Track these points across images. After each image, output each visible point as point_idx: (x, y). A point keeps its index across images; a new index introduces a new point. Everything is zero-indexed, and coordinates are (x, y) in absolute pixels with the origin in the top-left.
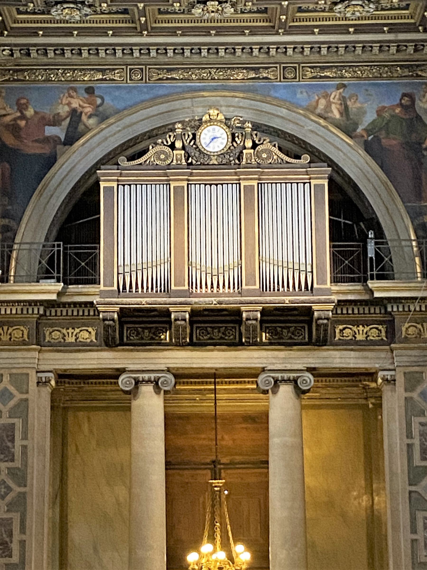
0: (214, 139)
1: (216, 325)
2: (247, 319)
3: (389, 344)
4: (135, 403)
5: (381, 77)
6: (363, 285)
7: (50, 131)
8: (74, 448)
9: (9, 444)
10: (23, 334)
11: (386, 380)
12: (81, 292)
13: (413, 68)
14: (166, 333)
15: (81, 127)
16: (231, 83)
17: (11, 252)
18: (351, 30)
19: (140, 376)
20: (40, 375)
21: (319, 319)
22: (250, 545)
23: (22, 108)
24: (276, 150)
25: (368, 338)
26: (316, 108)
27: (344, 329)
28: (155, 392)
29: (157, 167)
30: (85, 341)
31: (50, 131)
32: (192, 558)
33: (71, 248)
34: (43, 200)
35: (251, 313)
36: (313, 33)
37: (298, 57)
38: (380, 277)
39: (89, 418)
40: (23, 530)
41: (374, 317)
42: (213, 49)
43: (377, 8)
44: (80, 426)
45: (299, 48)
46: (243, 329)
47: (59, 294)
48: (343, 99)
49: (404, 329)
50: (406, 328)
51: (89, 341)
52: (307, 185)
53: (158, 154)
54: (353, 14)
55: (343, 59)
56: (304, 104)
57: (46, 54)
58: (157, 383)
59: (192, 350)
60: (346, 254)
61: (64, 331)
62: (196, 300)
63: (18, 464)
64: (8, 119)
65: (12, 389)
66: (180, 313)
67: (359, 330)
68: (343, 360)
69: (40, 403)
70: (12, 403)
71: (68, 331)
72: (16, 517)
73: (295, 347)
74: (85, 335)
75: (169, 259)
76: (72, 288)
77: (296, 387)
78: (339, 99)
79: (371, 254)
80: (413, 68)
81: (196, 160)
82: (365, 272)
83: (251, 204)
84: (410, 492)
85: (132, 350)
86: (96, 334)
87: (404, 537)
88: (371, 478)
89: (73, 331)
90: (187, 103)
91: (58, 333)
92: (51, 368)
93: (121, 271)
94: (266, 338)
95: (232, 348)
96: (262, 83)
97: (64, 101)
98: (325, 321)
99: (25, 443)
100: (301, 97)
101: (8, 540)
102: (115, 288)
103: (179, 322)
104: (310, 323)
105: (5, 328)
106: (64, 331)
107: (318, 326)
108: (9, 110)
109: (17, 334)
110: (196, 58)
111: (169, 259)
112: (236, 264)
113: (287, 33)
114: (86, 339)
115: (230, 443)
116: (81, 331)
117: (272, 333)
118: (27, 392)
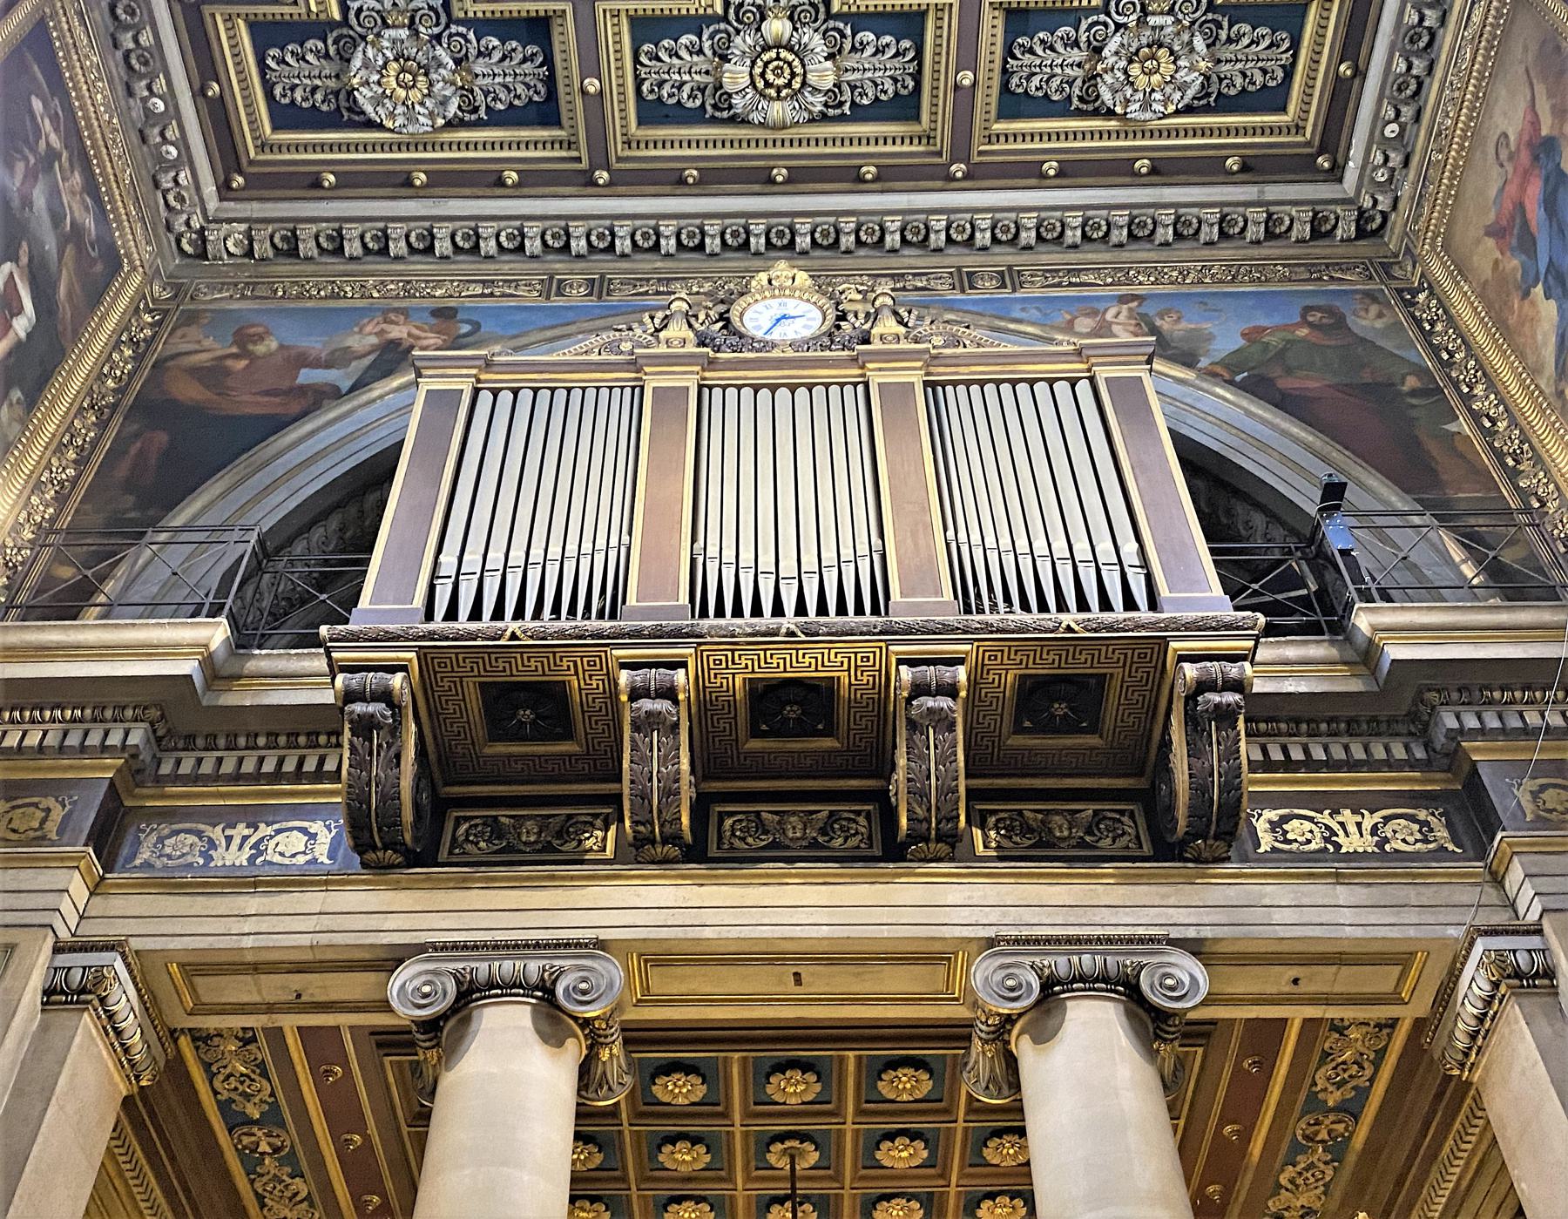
1: (796, 760)
2: (920, 689)
3: (1481, 855)
6: (1332, 642)
10: (44, 821)
12: (297, 678)
14: (607, 830)
20: (63, 960)
25: (1387, 847)
27: (1285, 819)
28: (538, 1032)
30: (287, 861)
47: (208, 662)
51: (301, 860)
67: (1342, 824)
71: (229, 832)
73: (1108, 868)
75: (625, 538)
78: (1130, 318)
89: (246, 832)
91: (191, 839)
94: (985, 847)
95: (857, 869)
98: (1231, 698)
103: (646, 705)
108: (208, 343)
111: (625, 538)
112: (863, 549)
114: (293, 856)
116: (278, 832)
117: (1009, 829)
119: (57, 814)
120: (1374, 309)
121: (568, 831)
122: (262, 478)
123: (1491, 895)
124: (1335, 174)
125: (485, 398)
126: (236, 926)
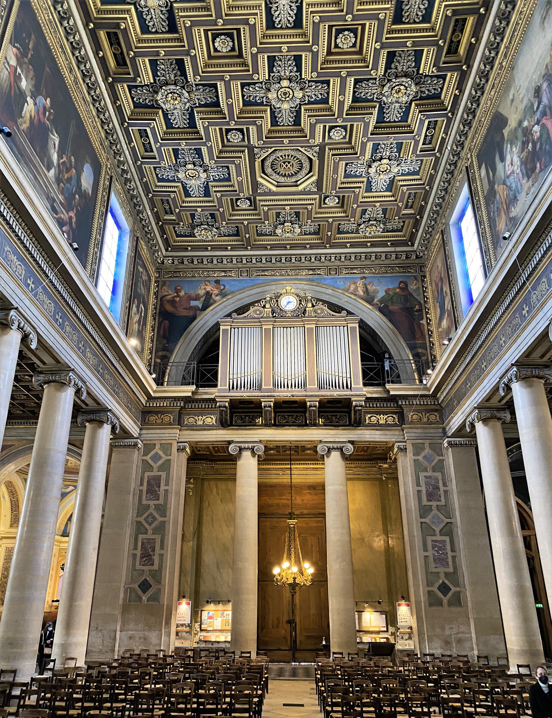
0: (289, 303)
1: (291, 412)
2: (310, 406)
3: (401, 426)
4: (239, 463)
5: (387, 273)
7: (193, 303)
8: (207, 503)
9: (157, 489)
11: (400, 449)
13: (405, 268)
15: (212, 301)
16: (299, 277)
17: (166, 368)
18: (369, 244)
19: (243, 445)
20: (179, 444)
21: (356, 406)
22: (314, 564)
23: (177, 291)
24: (326, 308)
26: (349, 289)
29: (255, 318)
31: (193, 303)
32: (276, 571)
33: (202, 366)
34: (187, 340)
35: (313, 403)
36: (346, 247)
37: (338, 263)
38: (393, 382)
39: (216, 486)
40: (162, 547)
41: (389, 410)
42: (289, 259)
43: (384, 230)
44: (212, 492)
45: (338, 257)
46: (307, 415)
47: (193, 393)
48: (365, 286)
49: (410, 416)
50: (410, 415)
52: (346, 328)
53: (255, 311)
54: (370, 233)
55: (364, 263)
56: (342, 287)
57: (193, 262)
58: (253, 450)
59: (275, 429)
60: (371, 370)
61: (196, 418)
62: (278, 394)
63: (161, 501)
64: (169, 297)
65: (160, 453)
66: (268, 403)
68: (371, 436)
69: (179, 464)
70: (160, 462)
72: (158, 537)
74: (209, 420)
76: (201, 390)
77: (343, 454)
79: (387, 368)
80: (405, 268)
81: (277, 313)
82: (384, 380)
83: (312, 339)
84: (421, 523)
85: (238, 429)
86: (216, 420)
87: (419, 554)
88: (387, 524)
90: (273, 287)
92: (187, 440)
93: (231, 377)
96: (317, 277)
97: (202, 287)
99: (166, 488)
100: (340, 283)
101: (152, 553)
102: (228, 387)
103: (267, 408)
104: (349, 413)
105: (159, 415)
106: (196, 418)
107: (355, 411)
109: (166, 419)
110: (279, 264)
113: (331, 247)
115: (300, 502)
118: (170, 455)
119: (172, 418)
120: (415, 282)
121: (253, 419)
122: (190, 336)
123: (401, 433)
124: (413, 245)
125: (233, 329)
126: (203, 437)
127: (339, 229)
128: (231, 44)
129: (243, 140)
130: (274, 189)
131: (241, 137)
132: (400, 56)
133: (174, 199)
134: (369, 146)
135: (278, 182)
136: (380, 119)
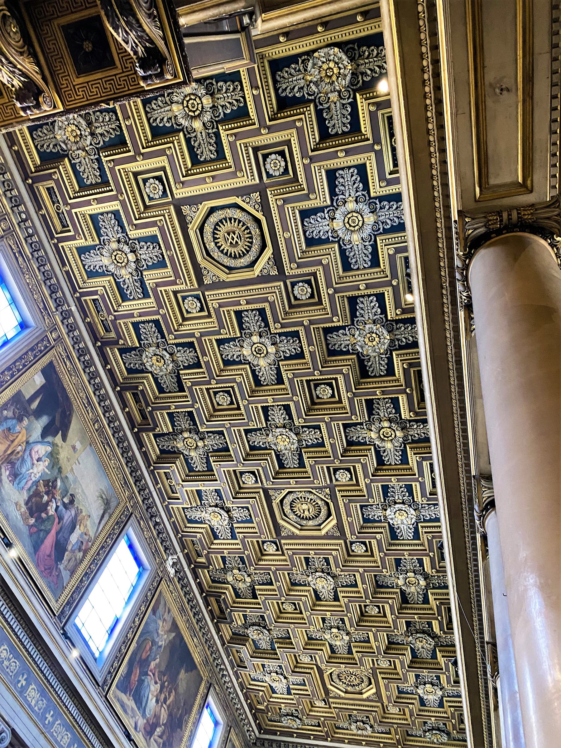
127: (377, 582)
128: (229, 398)
129: (256, 482)
130: (297, 532)
131: (254, 479)
132: (378, 404)
133: (200, 540)
134: (377, 487)
135: (301, 526)
136: (380, 461)
